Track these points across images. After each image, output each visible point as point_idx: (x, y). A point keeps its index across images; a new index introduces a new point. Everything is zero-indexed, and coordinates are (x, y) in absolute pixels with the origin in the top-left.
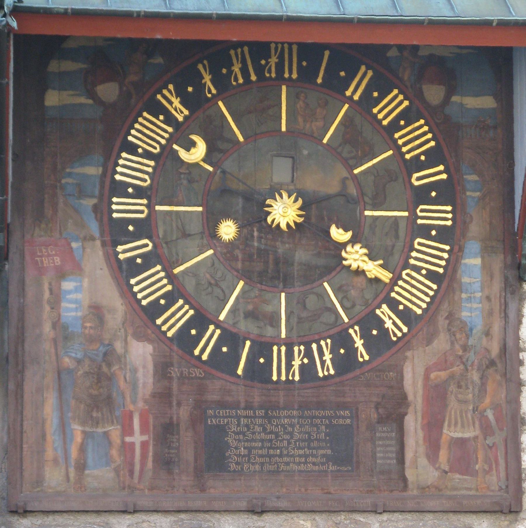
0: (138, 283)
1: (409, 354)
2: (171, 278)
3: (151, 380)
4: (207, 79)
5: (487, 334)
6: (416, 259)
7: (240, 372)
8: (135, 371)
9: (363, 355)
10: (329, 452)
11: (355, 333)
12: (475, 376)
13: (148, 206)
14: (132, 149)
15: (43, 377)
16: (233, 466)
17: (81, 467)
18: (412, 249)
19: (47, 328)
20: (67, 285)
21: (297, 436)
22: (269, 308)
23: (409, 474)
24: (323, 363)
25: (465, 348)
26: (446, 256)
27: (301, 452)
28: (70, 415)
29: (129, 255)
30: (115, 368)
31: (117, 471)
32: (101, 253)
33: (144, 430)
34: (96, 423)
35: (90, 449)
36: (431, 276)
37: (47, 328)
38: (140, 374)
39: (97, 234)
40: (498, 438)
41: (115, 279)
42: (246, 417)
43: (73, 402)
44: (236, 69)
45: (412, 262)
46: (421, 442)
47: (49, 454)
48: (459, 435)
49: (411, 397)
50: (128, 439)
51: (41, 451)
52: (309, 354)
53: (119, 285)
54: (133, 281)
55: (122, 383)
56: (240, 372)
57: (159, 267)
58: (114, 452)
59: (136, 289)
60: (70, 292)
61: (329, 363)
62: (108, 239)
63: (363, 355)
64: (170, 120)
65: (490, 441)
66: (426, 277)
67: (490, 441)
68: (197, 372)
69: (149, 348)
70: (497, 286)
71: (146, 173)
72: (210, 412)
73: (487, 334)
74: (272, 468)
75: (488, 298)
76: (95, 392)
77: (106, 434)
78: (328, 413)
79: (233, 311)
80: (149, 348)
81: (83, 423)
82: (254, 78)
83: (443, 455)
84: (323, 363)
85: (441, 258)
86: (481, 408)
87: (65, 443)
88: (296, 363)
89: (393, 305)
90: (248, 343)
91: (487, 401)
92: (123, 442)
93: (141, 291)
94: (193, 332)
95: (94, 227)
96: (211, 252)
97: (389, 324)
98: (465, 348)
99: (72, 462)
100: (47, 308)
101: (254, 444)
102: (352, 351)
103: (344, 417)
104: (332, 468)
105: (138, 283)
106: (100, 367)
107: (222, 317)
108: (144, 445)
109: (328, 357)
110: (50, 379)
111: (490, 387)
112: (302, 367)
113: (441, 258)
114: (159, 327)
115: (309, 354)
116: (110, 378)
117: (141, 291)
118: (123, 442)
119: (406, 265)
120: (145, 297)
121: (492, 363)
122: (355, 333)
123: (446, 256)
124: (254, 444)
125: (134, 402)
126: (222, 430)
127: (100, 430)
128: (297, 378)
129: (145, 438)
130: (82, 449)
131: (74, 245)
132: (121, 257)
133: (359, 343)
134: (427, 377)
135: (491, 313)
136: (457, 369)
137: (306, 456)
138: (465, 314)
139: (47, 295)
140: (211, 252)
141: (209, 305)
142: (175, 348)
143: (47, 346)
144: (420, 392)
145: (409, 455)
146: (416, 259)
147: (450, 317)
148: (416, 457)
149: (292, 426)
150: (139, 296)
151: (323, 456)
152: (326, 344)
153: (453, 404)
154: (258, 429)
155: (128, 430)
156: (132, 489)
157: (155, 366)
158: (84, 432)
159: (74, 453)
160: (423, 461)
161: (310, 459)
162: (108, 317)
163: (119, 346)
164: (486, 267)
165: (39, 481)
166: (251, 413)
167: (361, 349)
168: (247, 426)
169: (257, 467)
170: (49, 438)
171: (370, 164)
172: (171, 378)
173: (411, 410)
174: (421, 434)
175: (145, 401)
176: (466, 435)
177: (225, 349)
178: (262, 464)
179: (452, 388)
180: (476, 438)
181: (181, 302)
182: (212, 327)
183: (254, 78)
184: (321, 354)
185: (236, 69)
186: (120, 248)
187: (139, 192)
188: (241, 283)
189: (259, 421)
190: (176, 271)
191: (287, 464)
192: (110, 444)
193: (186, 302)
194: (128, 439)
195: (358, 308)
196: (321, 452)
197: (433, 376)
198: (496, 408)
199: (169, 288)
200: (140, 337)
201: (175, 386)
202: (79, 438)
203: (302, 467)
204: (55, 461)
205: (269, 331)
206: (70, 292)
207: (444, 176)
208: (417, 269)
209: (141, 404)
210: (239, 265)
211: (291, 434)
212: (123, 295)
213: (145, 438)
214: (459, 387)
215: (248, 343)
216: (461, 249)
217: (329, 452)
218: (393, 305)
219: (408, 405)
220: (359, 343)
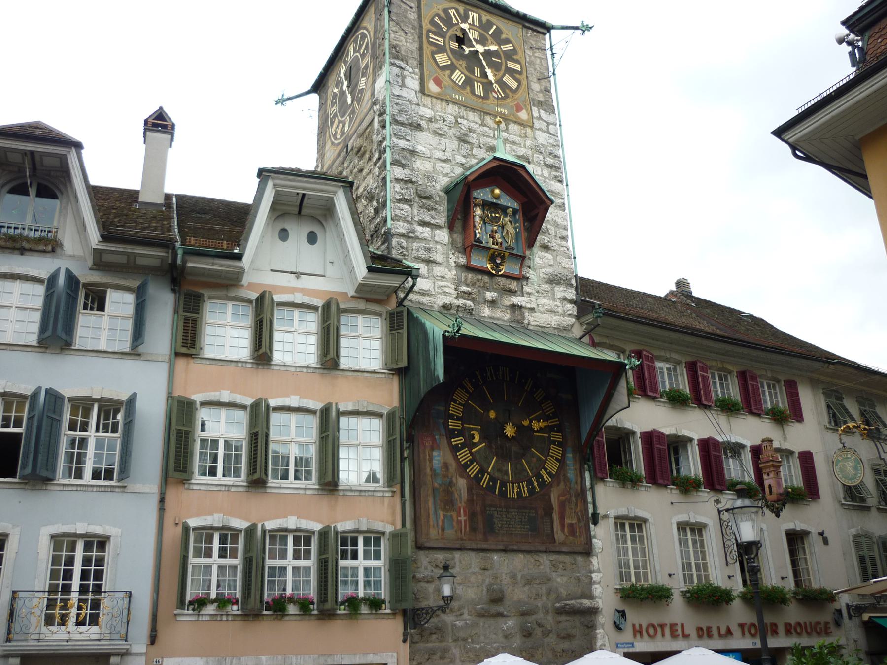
0: (459, 455)
1: (552, 489)
2: (470, 452)
3: (466, 494)
4: (479, 377)
5: (576, 483)
6: (552, 453)
7: (497, 493)
8: (460, 490)
9: (537, 489)
10: (528, 526)
11: (534, 479)
12: (573, 499)
13: (462, 424)
14: (455, 401)
15: (428, 490)
16: (497, 531)
17: (443, 529)
18: (550, 449)
19: (428, 470)
20: (435, 453)
21: (518, 520)
22: (504, 469)
23: (556, 537)
24: (524, 491)
25: (570, 488)
26: (561, 452)
27: (519, 526)
28: (438, 507)
29: (456, 443)
30: (453, 488)
31: (456, 531)
32: (446, 441)
33: (465, 515)
34: (447, 511)
35: (446, 520)
36: (557, 459)
37: (428, 470)
38: (462, 491)
39: (444, 434)
40: (582, 524)
41: (451, 451)
42: (500, 511)
43: (439, 502)
44: (489, 374)
45: (550, 454)
46: (558, 524)
47: (431, 523)
48: (570, 522)
49: (554, 506)
50: (459, 518)
51: (428, 521)
52: (519, 487)
53: (453, 455)
54: (458, 454)
55: (456, 495)
56: (497, 493)
57: (467, 449)
58: (455, 524)
59: (459, 457)
60: (436, 456)
61: (526, 491)
62: (448, 436)
63: (537, 489)
64: (467, 392)
65: (580, 525)
66: (555, 460)
67: (580, 525)
68: (482, 492)
69: (465, 481)
70: (578, 466)
71: (460, 411)
72: (488, 508)
73: (576, 483)
74: (510, 532)
75: (576, 469)
76: (446, 498)
77: (451, 516)
78: (527, 511)
79: (493, 468)
80: (465, 481)
81: (443, 511)
82: (495, 379)
83: (566, 530)
84: (524, 491)
85: (560, 453)
86: (576, 511)
87: (437, 518)
88: (515, 490)
89: (546, 470)
90: (499, 482)
91: (578, 509)
92: (458, 519)
93: (461, 458)
94: (480, 476)
95: (443, 431)
96: (484, 444)
97: (545, 477)
98: (570, 488)
99: (440, 527)
100: (428, 463)
101: (503, 522)
102: (534, 487)
103: (533, 513)
104: (530, 533)
105: (459, 455)
106: (448, 488)
107: (489, 470)
108: (465, 521)
109: (526, 489)
110: (430, 491)
111: (579, 503)
112: (517, 492)
113: (560, 453)
114: (468, 473)
115: (519, 487)
116: (452, 493)
117: (461, 458)
118: (458, 519)
119: (549, 455)
120: (463, 461)
121: (578, 495)
122: (534, 479)
123: (561, 452)
124: (503, 522)
125: (461, 503)
126: (492, 516)
127: (449, 514)
128: (516, 496)
129: (465, 518)
130: (443, 521)
131: (436, 437)
132: (453, 443)
133: (536, 484)
134: (558, 499)
135: (576, 475)
136: (568, 496)
137: (521, 528)
138: (569, 475)
139: (428, 457)
140: (484, 444)
141: (485, 466)
142: (474, 481)
143: (429, 478)
144: (557, 504)
145: (555, 530)
146: (552, 453)
147: (565, 476)
148: (557, 532)
149: (516, 516)
150: (461, 460)
151: (527, 528)
152: (525, 483)
153: (567, 508)
154: (504, 516)
155: (459, 515)
156: (462, 540)
157: (467, 489)
158: (444, 516)
159: (440, 523)
160: (560, 532)
161: (523, 529)
162: (450, 467)
163: (454, 479)
164: (574, 457)
165: (428, 534)
166: (501, 509)
167: (536, 486)
168: (500, 515)
169: (505, 532)
170: (431, 516)
171: (534, 416)
172: (473, 494)
173: (554, 511)
174: (558, 521)
175: (465, 503)
176: (573, 522)
177: (491, 483)
178: (506, 531)
179: (567, 503)
180: (576, 523)
181: (475, 463)
182: (486, 474)
183: (495, 379)
184: (524, 488)
185: (489, 374)
186: (453, 440)
187: (458, 419)
188: (495, 457)
189: (504, 513)
190: (473, 450)
191: (515, 531)
192: (453, 520)
193: (477, 463)
194: (459, 518)
195: (534, 470)
196: (526, 527)
197: (561, 498)
198: (581, 511)
199: (471, 457)
200: (462, 477)
201: (475, 497)
202: (442, 517)
203: (520, 532)
204: (433, 526)
205: (506, 478)
206: (436, 456)
207: (558, 422)
208: (553, 457)
209: (463, 504)
210: (494, 450)
211: (515, 518)
212: (454, 459)
213: (465, 518)
214: (569, 503)
215: (499, 482)
216: (565, 450)
217: (528, 526)
218: (546, 470)
219: (553, 509)
220: (536, 484)
